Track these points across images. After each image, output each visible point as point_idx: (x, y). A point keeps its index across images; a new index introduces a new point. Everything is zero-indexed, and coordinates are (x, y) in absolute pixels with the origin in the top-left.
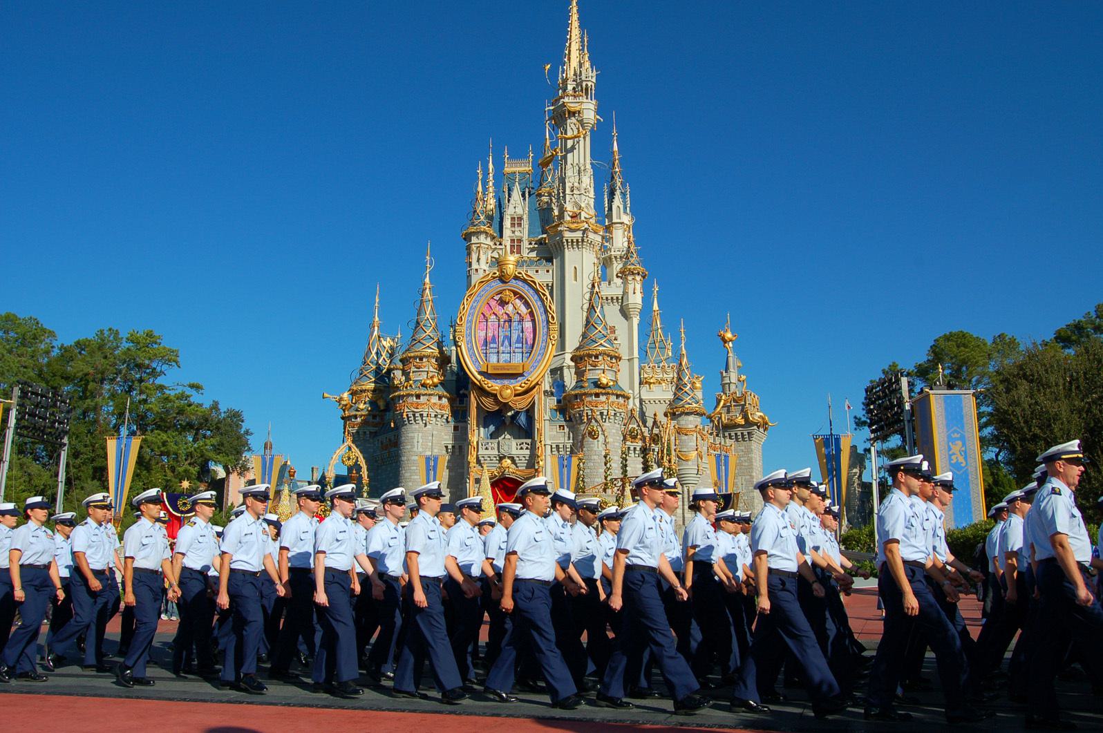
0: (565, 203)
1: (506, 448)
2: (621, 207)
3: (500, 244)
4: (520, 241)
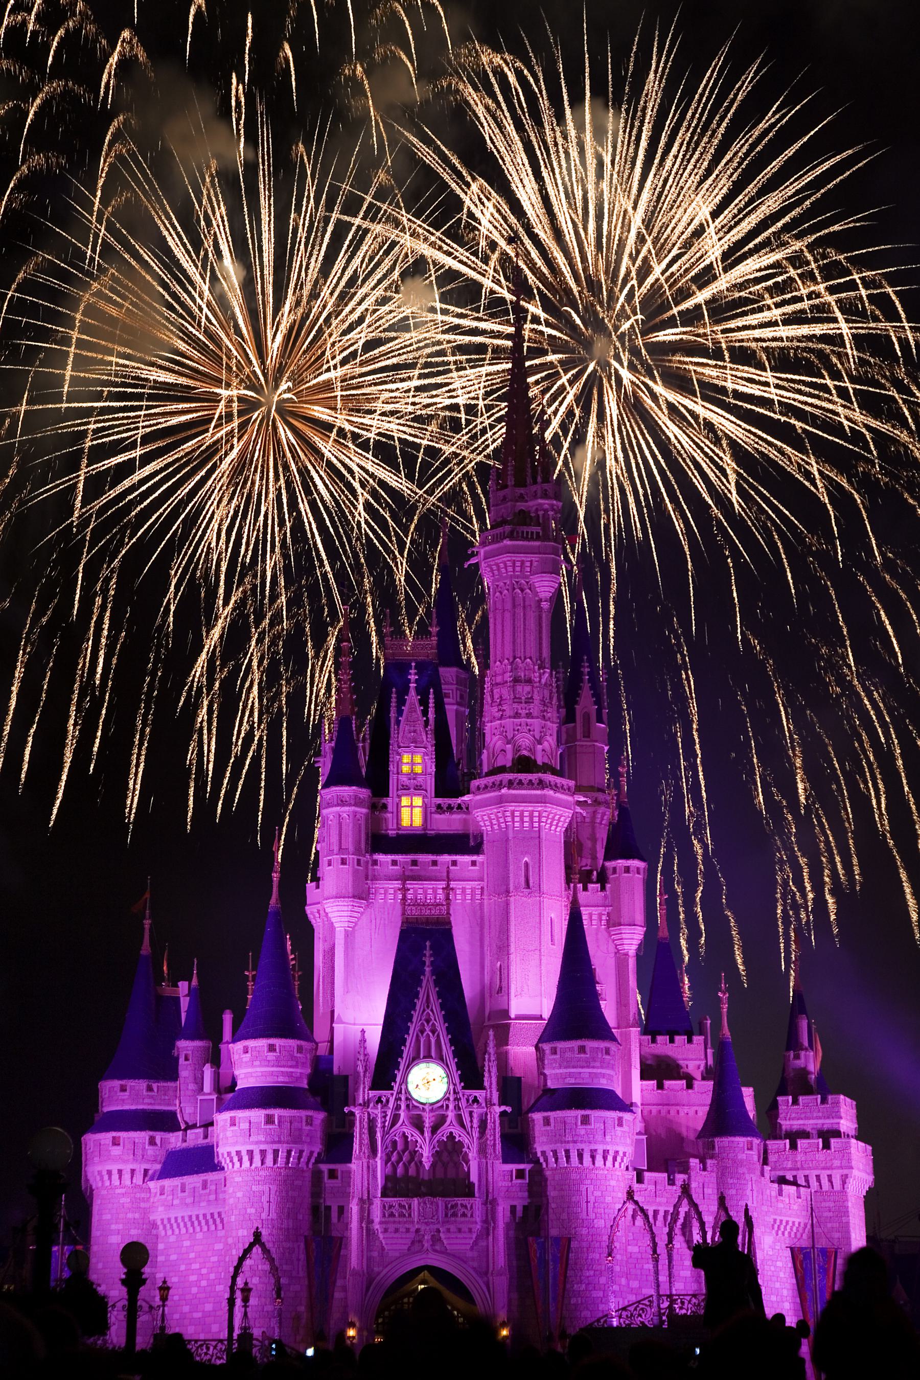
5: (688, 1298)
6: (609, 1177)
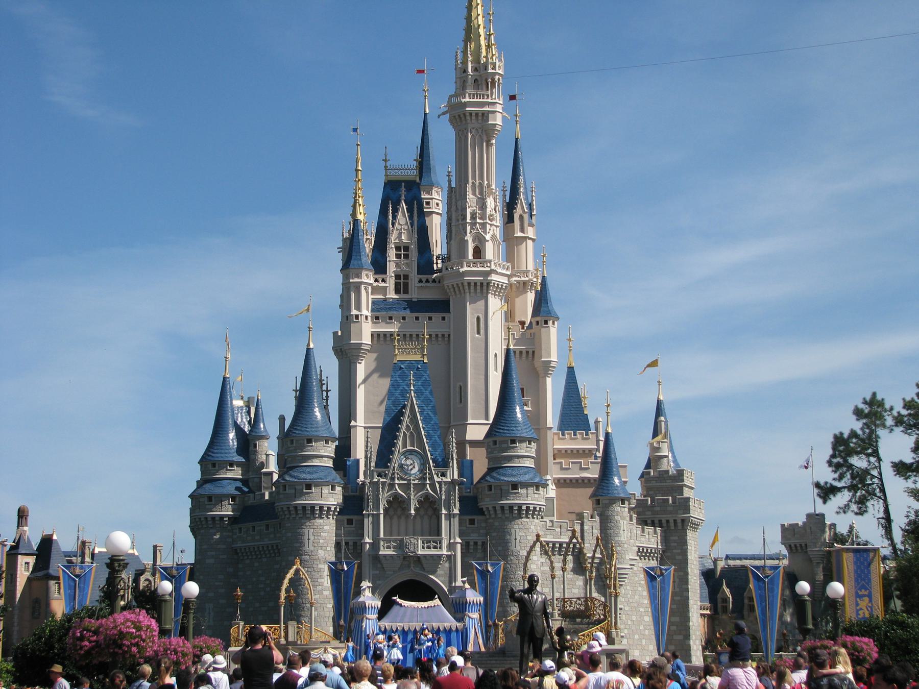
0: (466, 233)
1: (412, 548)
2: (526, 217)
3: (383, 281)
4: (406, 277)
5: (575, 600)
6: (529, 523)
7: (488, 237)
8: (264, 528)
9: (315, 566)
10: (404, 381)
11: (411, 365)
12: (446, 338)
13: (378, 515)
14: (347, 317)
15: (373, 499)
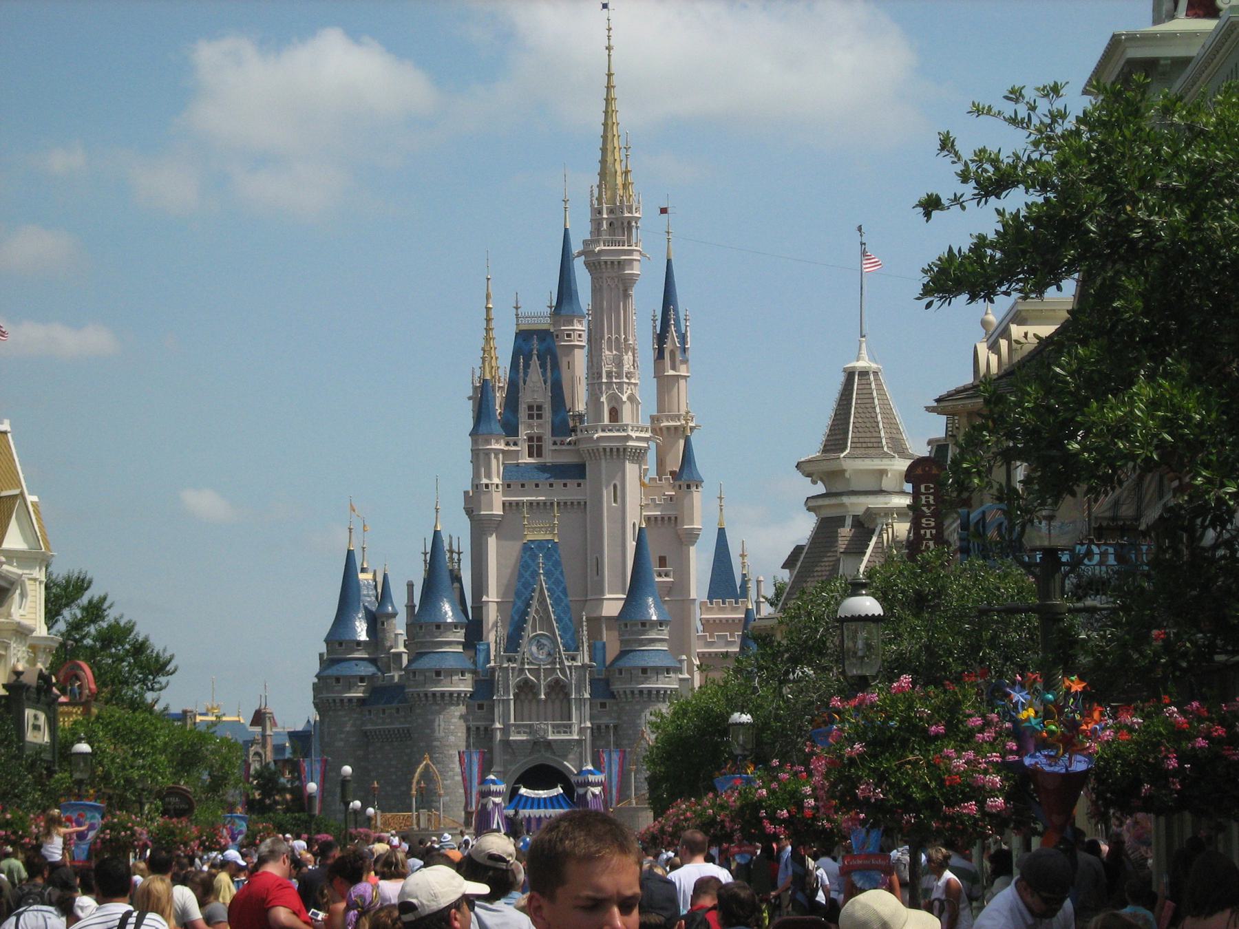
0: (601, 393)
1: (542, 733)
3: (515, 444)
4: (539, 439)
7: (624, 398)
8: (394, 711)
9: (445, 752)
10: (534, 561)
11: (541, 544)
12: (582, 506)
13: (509, 700)
14: (477, 486)
15: (503, 684)
